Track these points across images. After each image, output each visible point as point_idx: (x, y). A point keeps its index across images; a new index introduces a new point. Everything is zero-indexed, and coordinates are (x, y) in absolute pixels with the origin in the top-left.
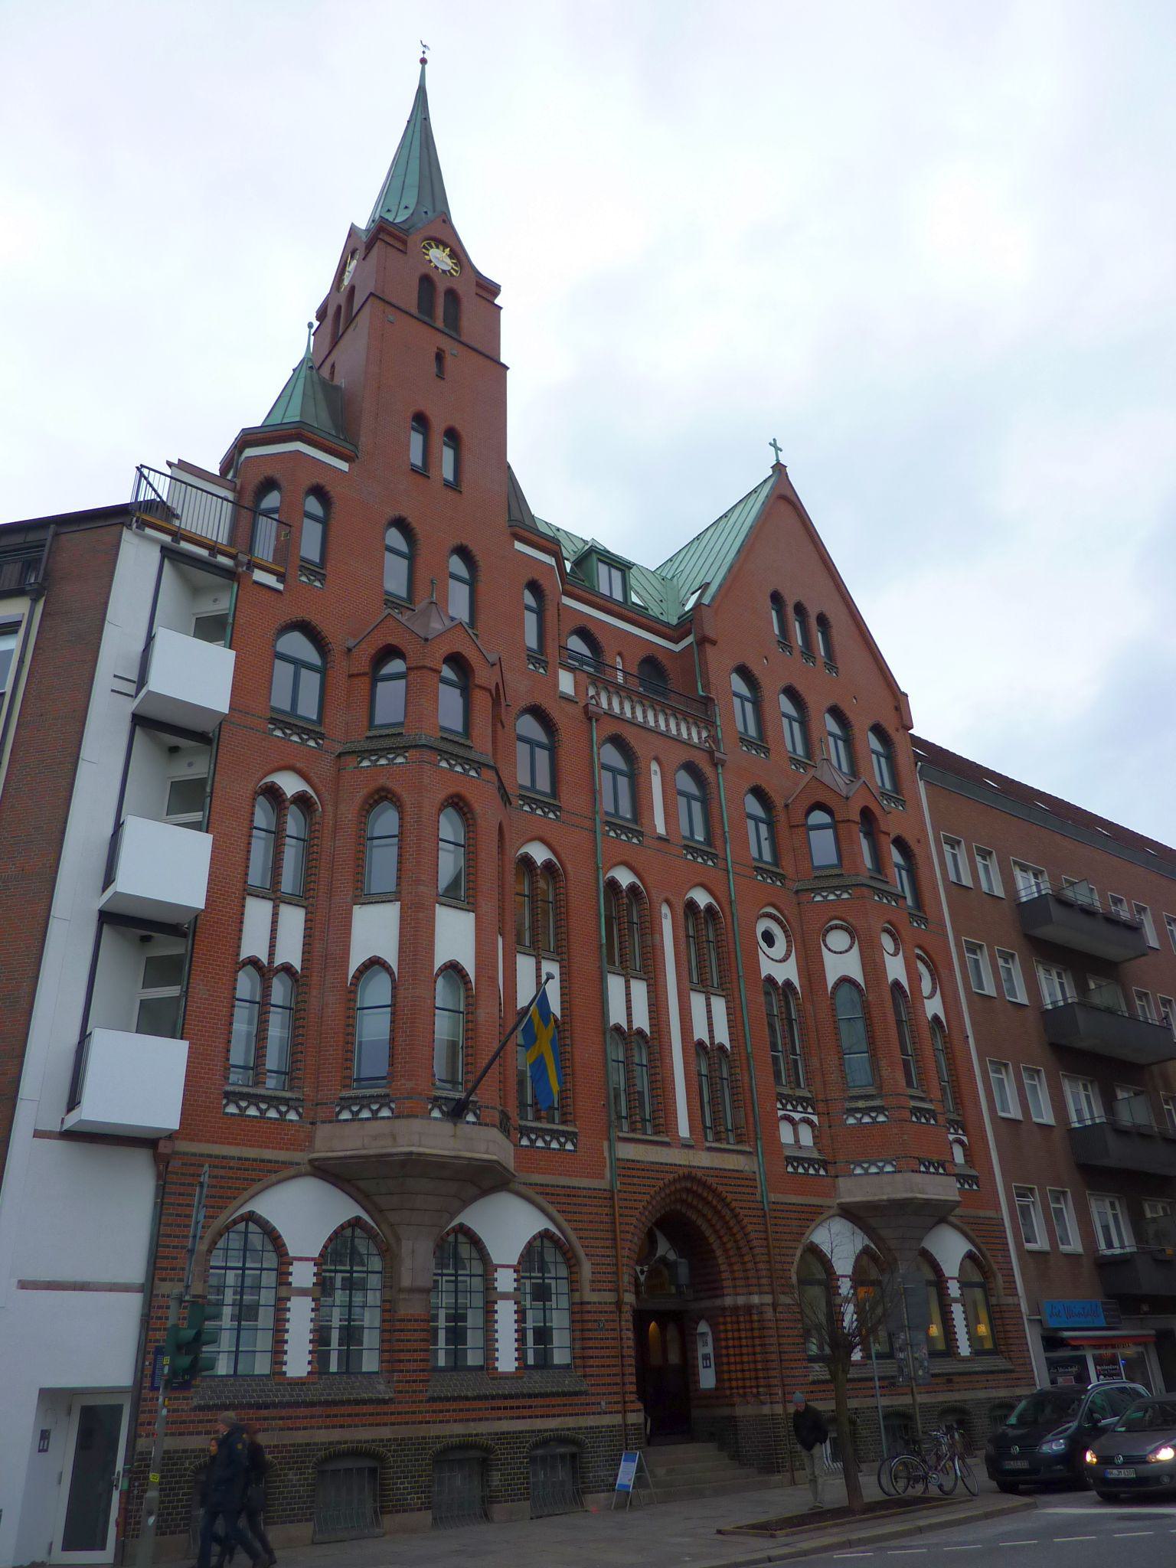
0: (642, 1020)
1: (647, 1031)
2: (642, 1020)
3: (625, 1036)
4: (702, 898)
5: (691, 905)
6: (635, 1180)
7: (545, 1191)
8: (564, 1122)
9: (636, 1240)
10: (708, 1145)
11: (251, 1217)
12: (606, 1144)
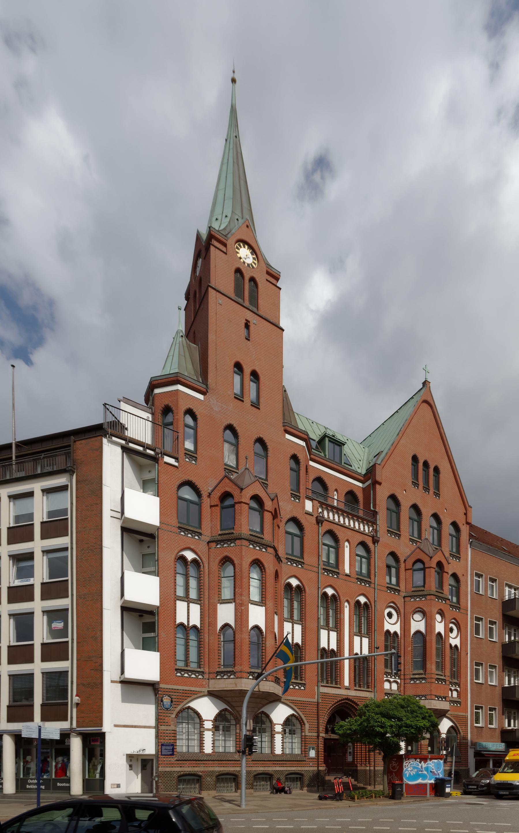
0: (333, 646)
1: (335, 649)
2: (333, 646)
3: (325, 652)
4: (362, 600)
5: (358, 602)
6: (326, 699)
7: (294, 702)
8: (301, 680)
9: (326, 717)
10: (356, 688)
11: (189, 708)
12: (316, 687)
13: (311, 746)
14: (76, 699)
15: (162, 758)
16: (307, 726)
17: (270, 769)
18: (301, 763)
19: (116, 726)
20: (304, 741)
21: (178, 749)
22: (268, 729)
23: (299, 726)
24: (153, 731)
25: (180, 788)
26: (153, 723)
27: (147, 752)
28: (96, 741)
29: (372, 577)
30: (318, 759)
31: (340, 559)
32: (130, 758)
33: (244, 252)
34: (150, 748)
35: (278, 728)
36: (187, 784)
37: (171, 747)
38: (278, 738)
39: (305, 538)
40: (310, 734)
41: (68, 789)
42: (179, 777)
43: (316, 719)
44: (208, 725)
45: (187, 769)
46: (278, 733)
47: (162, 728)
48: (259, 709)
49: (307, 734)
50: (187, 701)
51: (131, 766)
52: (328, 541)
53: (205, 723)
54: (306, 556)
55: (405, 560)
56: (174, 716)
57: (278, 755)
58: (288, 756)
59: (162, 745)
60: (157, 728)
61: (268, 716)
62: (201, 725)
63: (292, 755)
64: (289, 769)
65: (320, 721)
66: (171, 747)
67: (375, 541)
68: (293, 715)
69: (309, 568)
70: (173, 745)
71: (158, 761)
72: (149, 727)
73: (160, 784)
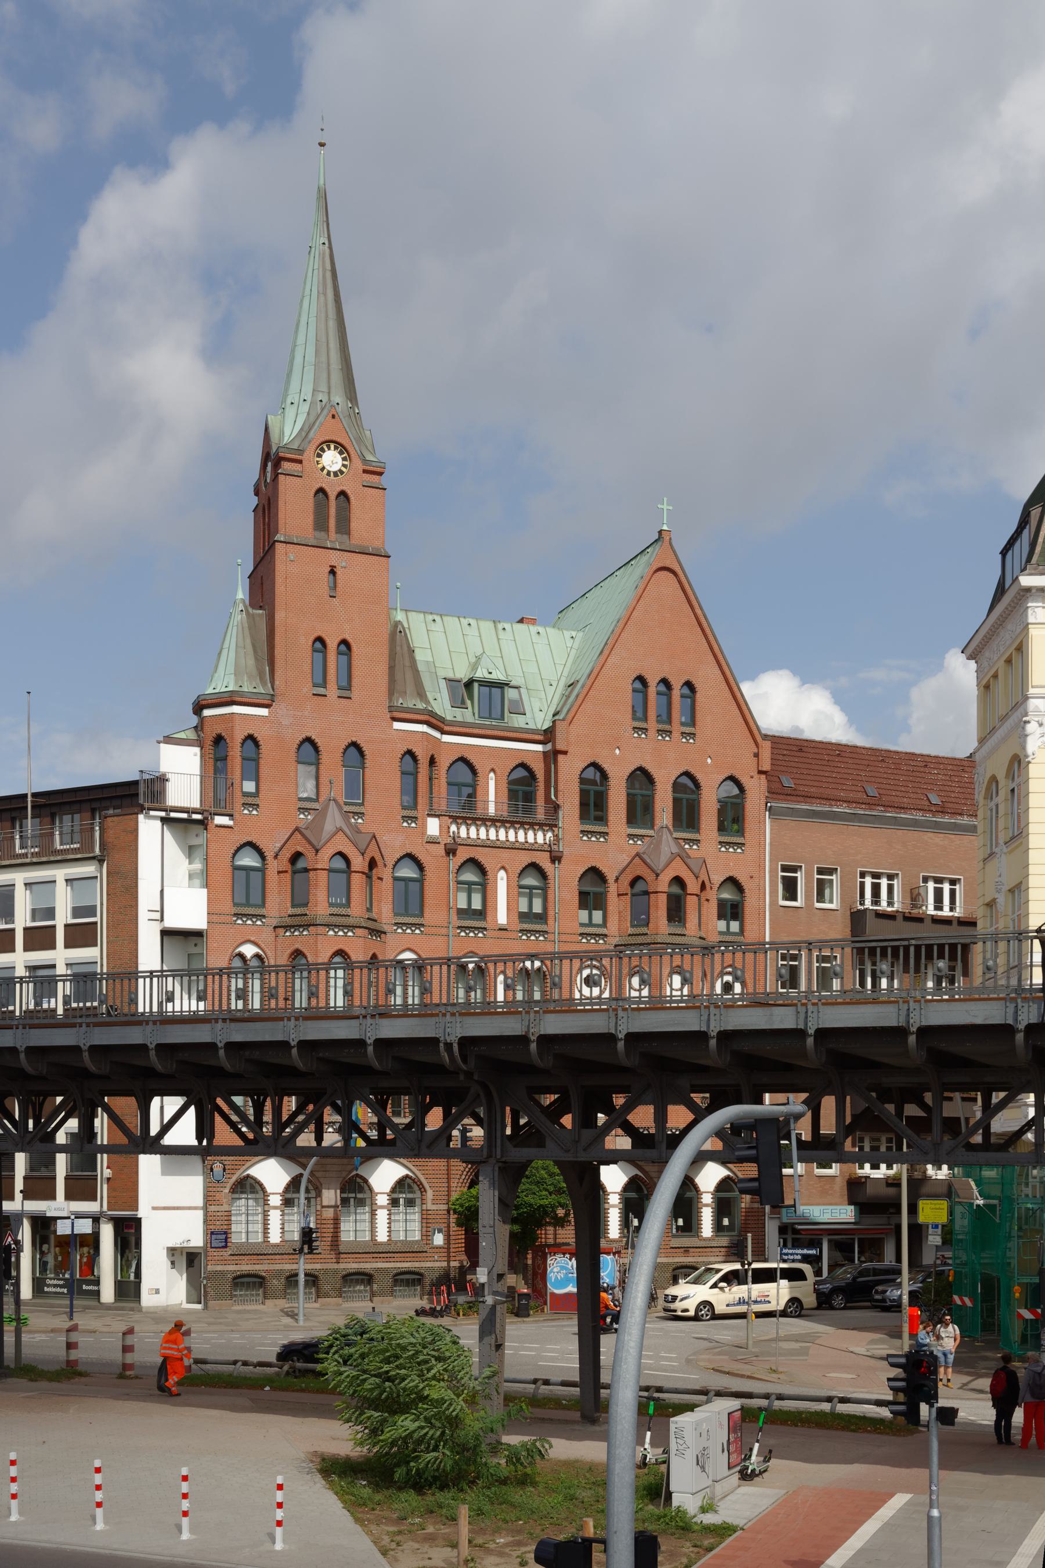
11: (248, 1176)
13: (437, 1226)
14: (107, 1173)
15: (212, 1252)
16: (430, 1194)
17: (368, 1266)
18: (420, 1255)
19: (154, 1208)
20: (426, 1218)
21: (234, 1239)
22: (368, 1202)
23: (418, 1194)
24: (200, 1214)
25: (235, 1296)
26: (200, 1202)
27: (192, 1244)
28: (130, 1227)
29: (550, 921)
30: (448, 1248)
31: (489, 904)
32: (172, 1251)
33: (331, 459)
34: (197, 1240)
35: (382, 1200)
36: (247, 1290)
37: (224, 1236)
38: (382, 1216)
39: (426, 883)
40: (434, 1207)
41: (98, 1293)
42: (235, 1278)
43: (445, 1180)
44: (275, 1200)
45: (246, 1267)
46: (382, 1207)
47: (212, 1208)
48: (350, 1172)
49: (430, 1206)
50: (244, 1167)
51: (173, 1263)
52: (469, 876)
53: (271, 1198)
54: (427, 911)
55: (617, 880)
56: (227, 1191)
57: (381, 1244)
58: (399, 1244)
59: (212, 1233)
60: (205, 1208)
61: (366, 1181)
62: (266, 1202)
63: (405, 1242)
64: (399, 1265)
65: (452, 1185)
66: (224, 1236)
67: (556, 858)
68: (407, 1176)
69: (433, 930)
70: (226, 1233)
71: (206, 1256)
72: (195, 1208)
73: (209, 1290)
